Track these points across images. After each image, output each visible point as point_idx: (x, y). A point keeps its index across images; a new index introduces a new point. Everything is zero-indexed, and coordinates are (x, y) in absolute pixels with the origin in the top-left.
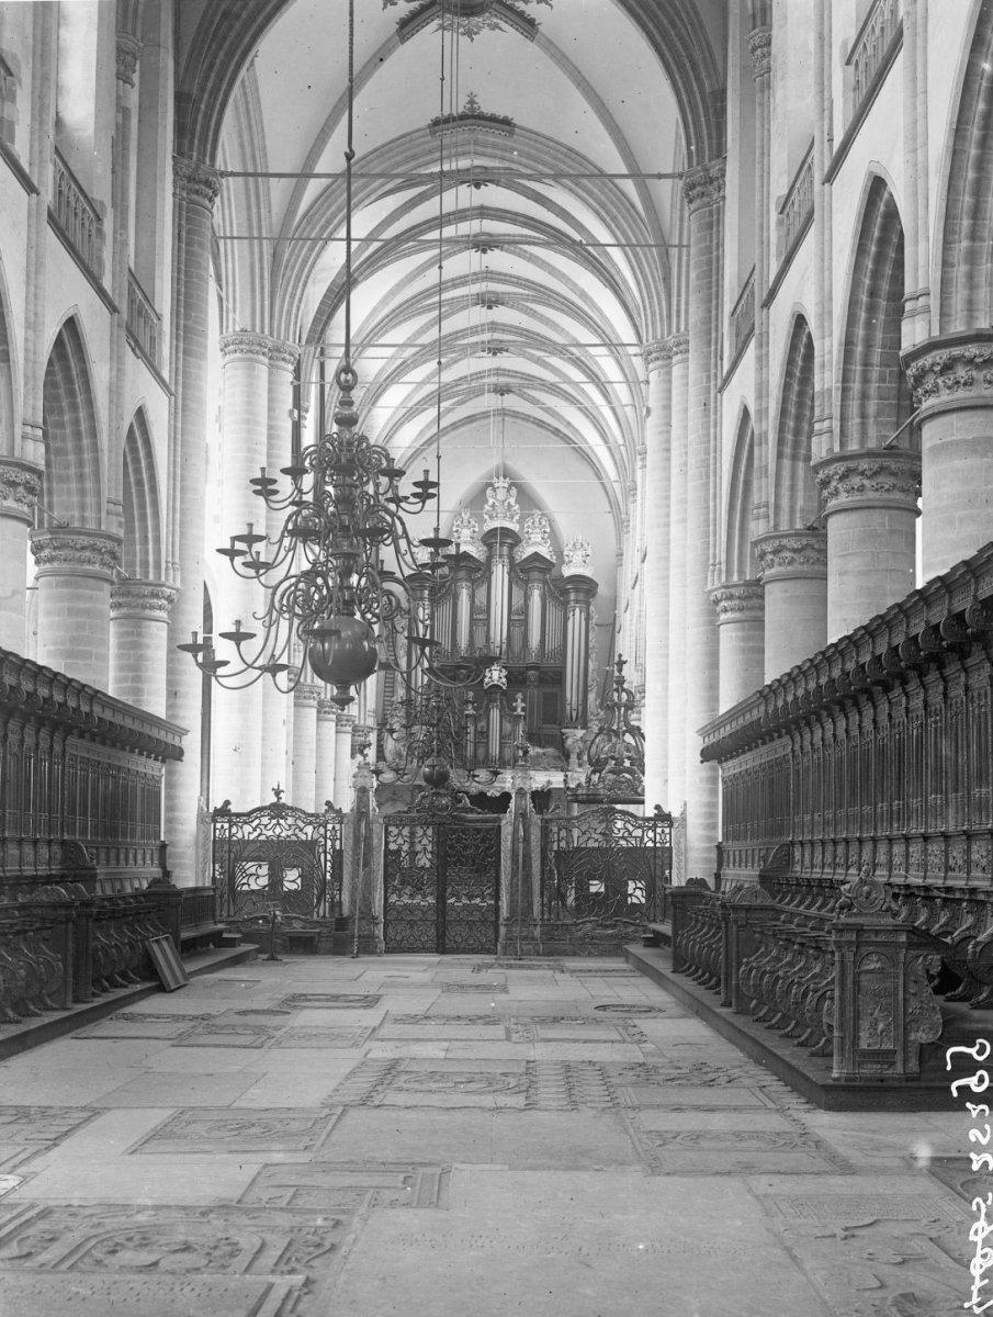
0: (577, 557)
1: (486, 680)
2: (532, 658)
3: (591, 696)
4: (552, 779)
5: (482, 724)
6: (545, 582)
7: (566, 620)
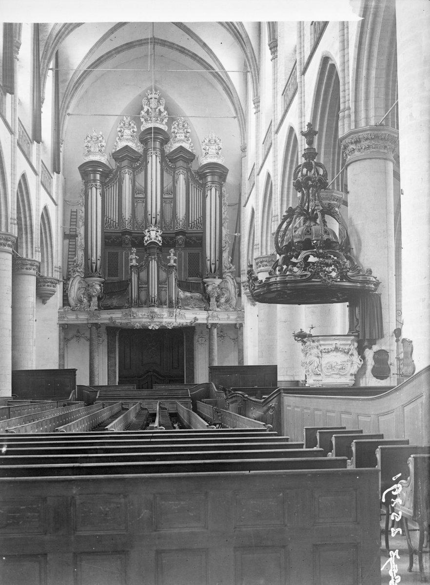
0: (212, 150)
1: (146, 238)
2: (180, 226)
3: (225, 255)
4: (198, 317)
5: (143, 274)
6: (188, 170)
7: (205, 197)
